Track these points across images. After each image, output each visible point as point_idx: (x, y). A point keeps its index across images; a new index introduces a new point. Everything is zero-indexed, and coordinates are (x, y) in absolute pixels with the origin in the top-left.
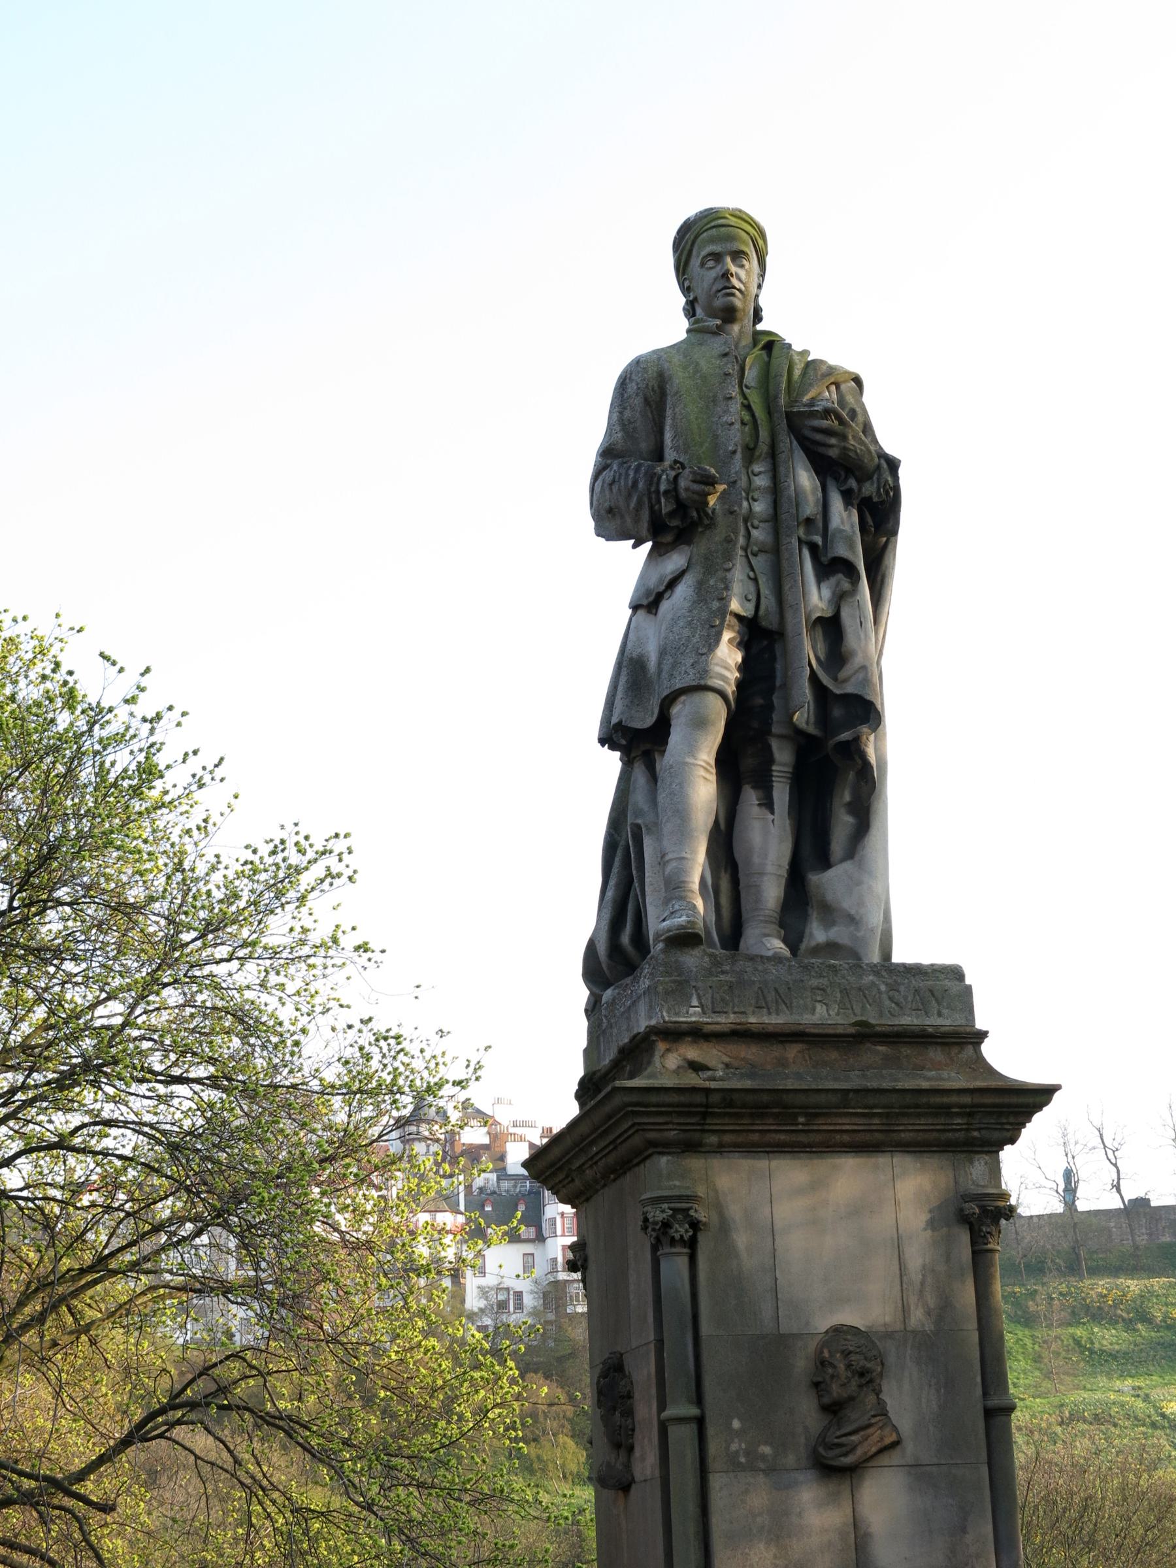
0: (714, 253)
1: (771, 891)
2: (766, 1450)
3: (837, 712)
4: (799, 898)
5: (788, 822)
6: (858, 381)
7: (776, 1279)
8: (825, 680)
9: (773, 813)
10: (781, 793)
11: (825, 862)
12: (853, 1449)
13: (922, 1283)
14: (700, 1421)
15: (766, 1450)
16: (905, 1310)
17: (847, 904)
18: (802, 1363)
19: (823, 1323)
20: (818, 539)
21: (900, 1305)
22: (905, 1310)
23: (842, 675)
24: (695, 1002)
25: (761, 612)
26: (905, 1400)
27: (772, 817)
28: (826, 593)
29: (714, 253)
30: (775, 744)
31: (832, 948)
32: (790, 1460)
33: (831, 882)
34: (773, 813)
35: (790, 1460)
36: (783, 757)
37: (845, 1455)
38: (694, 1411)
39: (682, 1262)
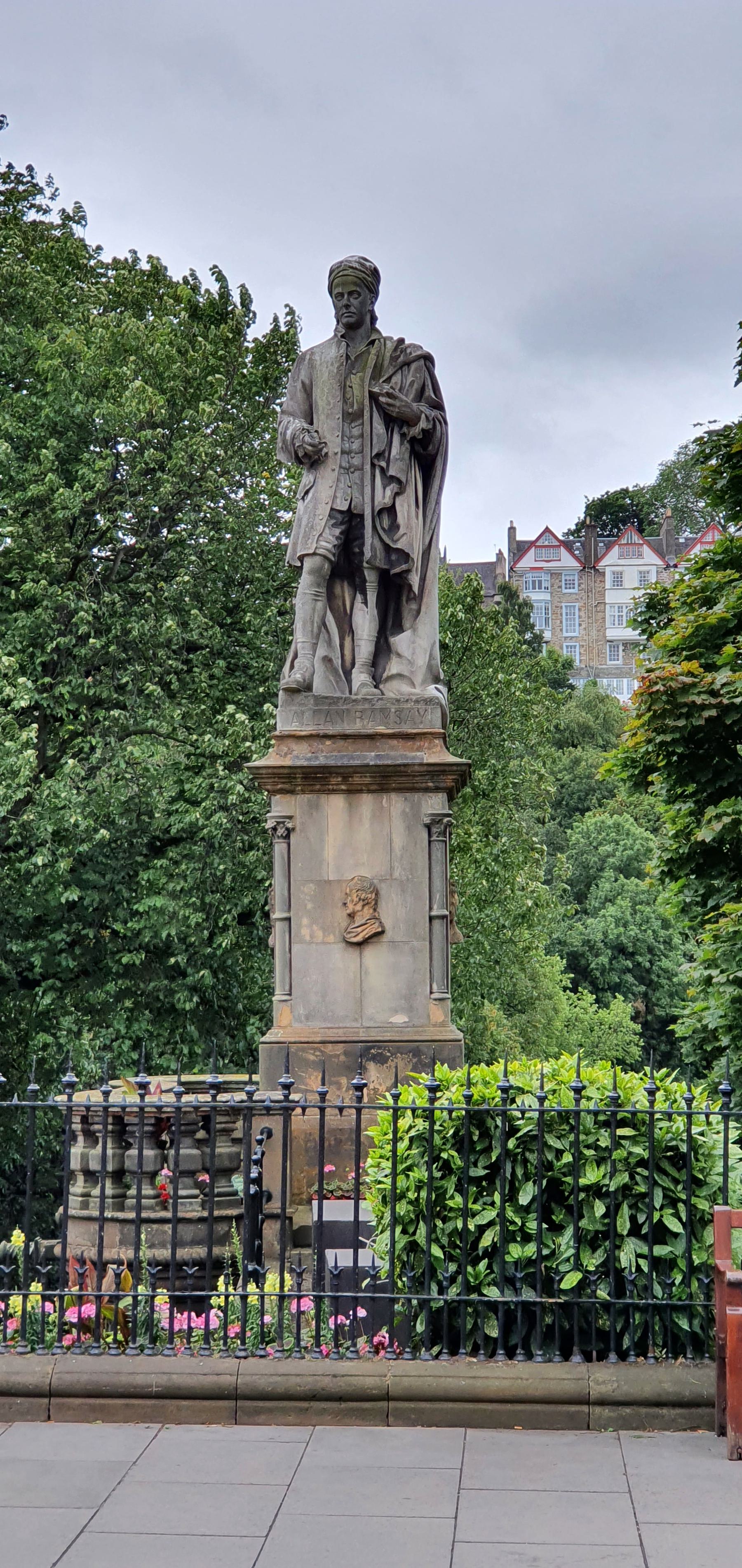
1: (365, 649)
3: (394, 557)
4: (383, 648)
6: (428, 359)
10: (372, 597)
11: (399, 628)
14: (289, 919)
20: (383, 464)
23: (395, 538)
28: (388, 492)
30: (366, 573)
31: (400, 676)
33: (400, 641)
36: (371, 577)
38: (285, 915)
39: (285, 845)
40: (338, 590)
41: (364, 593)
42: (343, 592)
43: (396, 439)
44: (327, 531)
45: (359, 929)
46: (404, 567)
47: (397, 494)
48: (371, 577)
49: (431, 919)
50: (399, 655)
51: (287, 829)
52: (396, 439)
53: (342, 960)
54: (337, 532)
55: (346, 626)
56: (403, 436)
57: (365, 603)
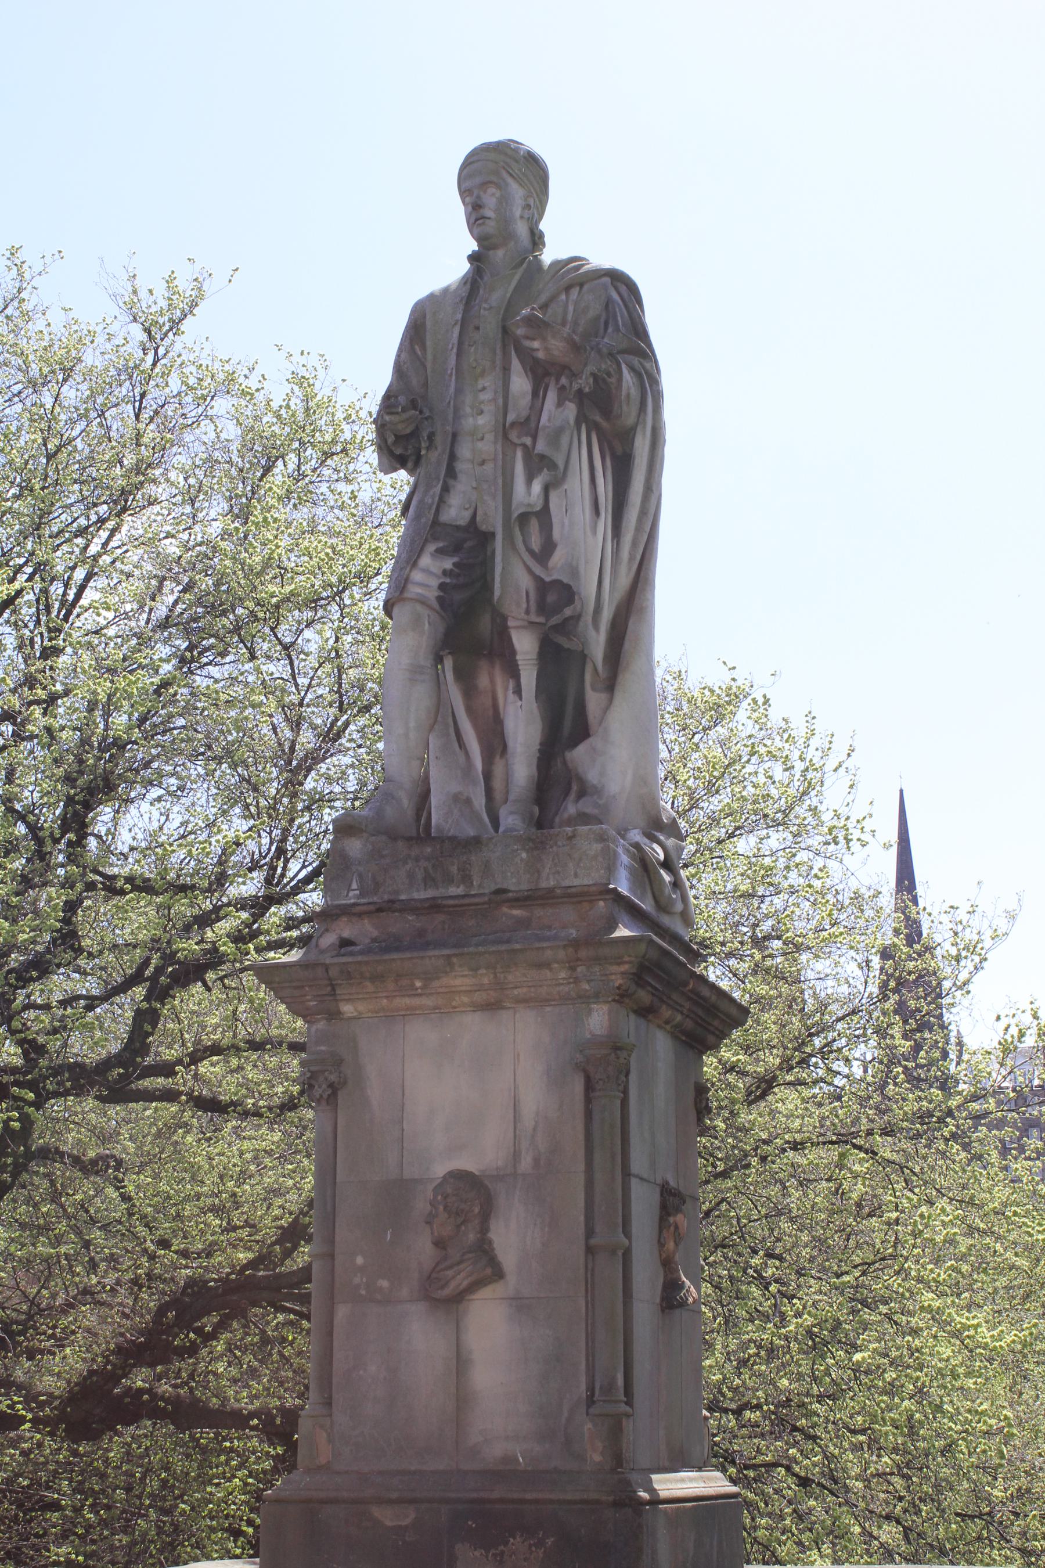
0: (502, 183)
2: (384, 1283)
3: (551, 598)
5: (535, 705)
7: (403, 1130)
8: (538, 570)
9: (521, 699)
12: (447, 1283)
13: (535, 1129)
15: (384, 1283)
16: (516, 1155)
17: (592, 776)
18: (421, 1205)
19: (440, 1170)
20: (528, 441)
21: (512, 1150)
22: (516, 1155)
23: (551, 564)
24: (354, 886)
25: (478, 519)
26: (512, 1236)
27: (520, 703)
28: (537, 487)
29: (502, 183)
32: (405, 1292)
34: (521, 699)
35: (405, 1292)
37: (442, 1288)
40: (483, 681)
41: (513, 671)
42: (492, 682)
43: (552, 397)
44: (426, 560)
45: (450, 1273)
46: (568, 612)
47: (546, 489)
48: (525, 645)
49: (590, 1250)
50: (582, 781)
51: (331, 1085)
52: (552, 397)
53: (422, 1336)
54: (448, 564)
55: (495, 743)
56: (562, 389)
57: (518, 691)
